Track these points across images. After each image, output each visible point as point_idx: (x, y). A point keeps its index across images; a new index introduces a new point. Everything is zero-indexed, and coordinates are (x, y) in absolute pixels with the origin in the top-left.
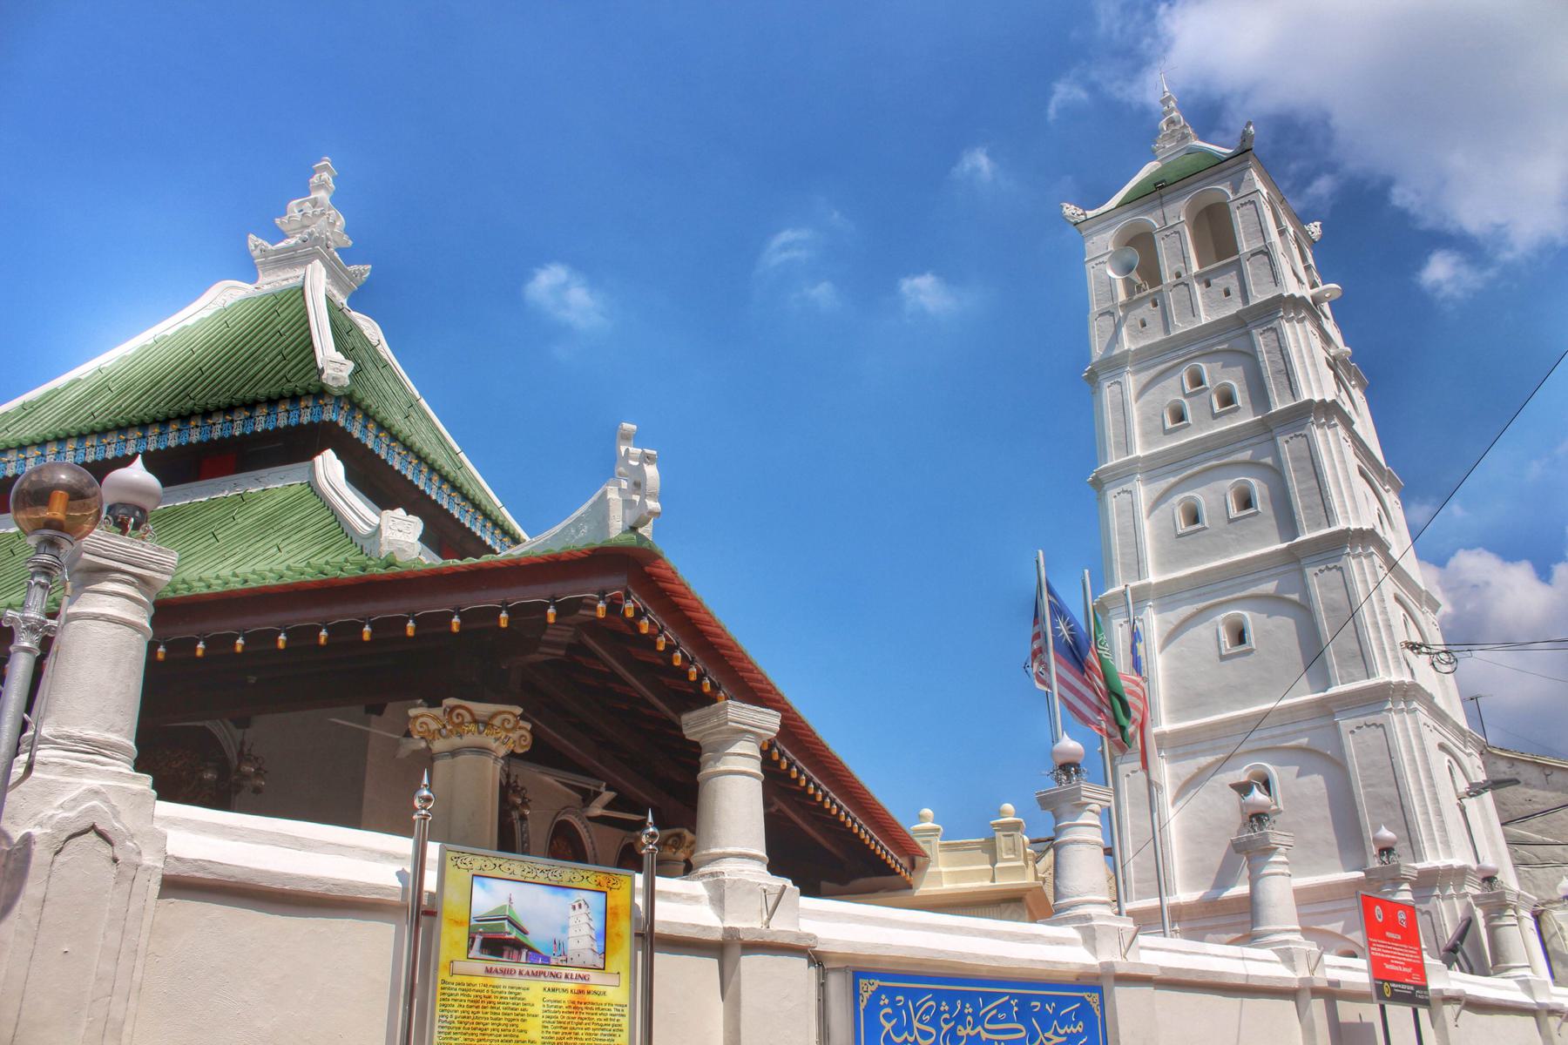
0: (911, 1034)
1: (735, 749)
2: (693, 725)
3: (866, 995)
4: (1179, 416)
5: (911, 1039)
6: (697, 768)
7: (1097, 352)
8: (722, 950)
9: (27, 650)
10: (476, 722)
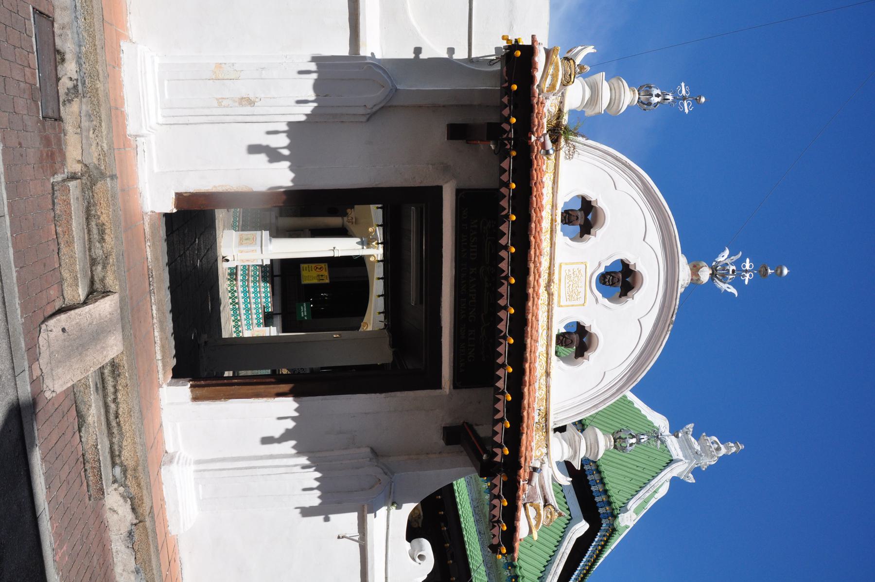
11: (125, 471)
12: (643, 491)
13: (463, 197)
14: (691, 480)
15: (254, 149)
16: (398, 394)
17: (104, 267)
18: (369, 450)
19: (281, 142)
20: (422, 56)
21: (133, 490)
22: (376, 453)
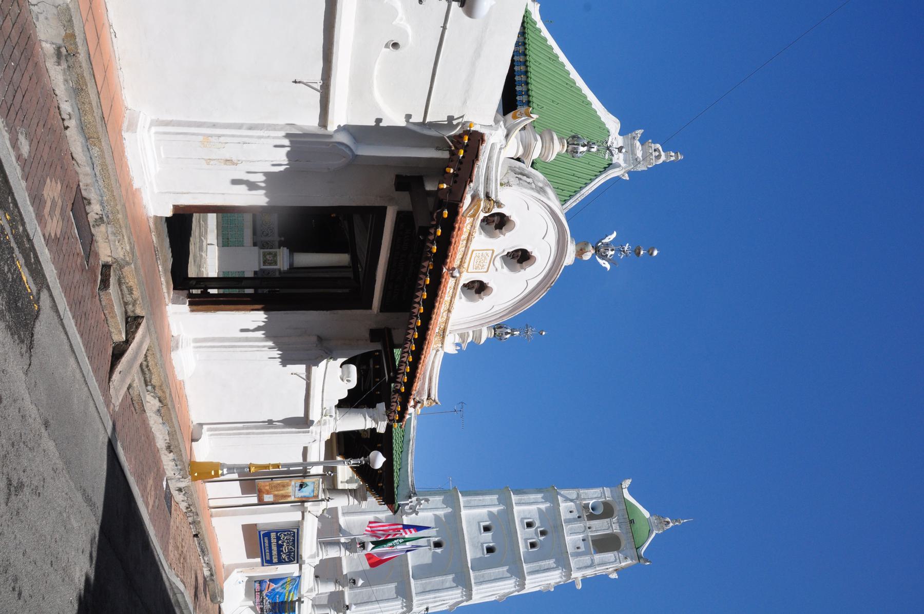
4: (529, 525)
7: (562, 492)
11: (154, 387)
12: (571, 201)
13: (403, 219)
14: (626, 177)
15: (235, 182)
16: (340, 312)
17: (134, 305)
18: (314, 339)
19: (260, 178)
20: (381, 125)
21: (160, 394)
22: (320, 339)
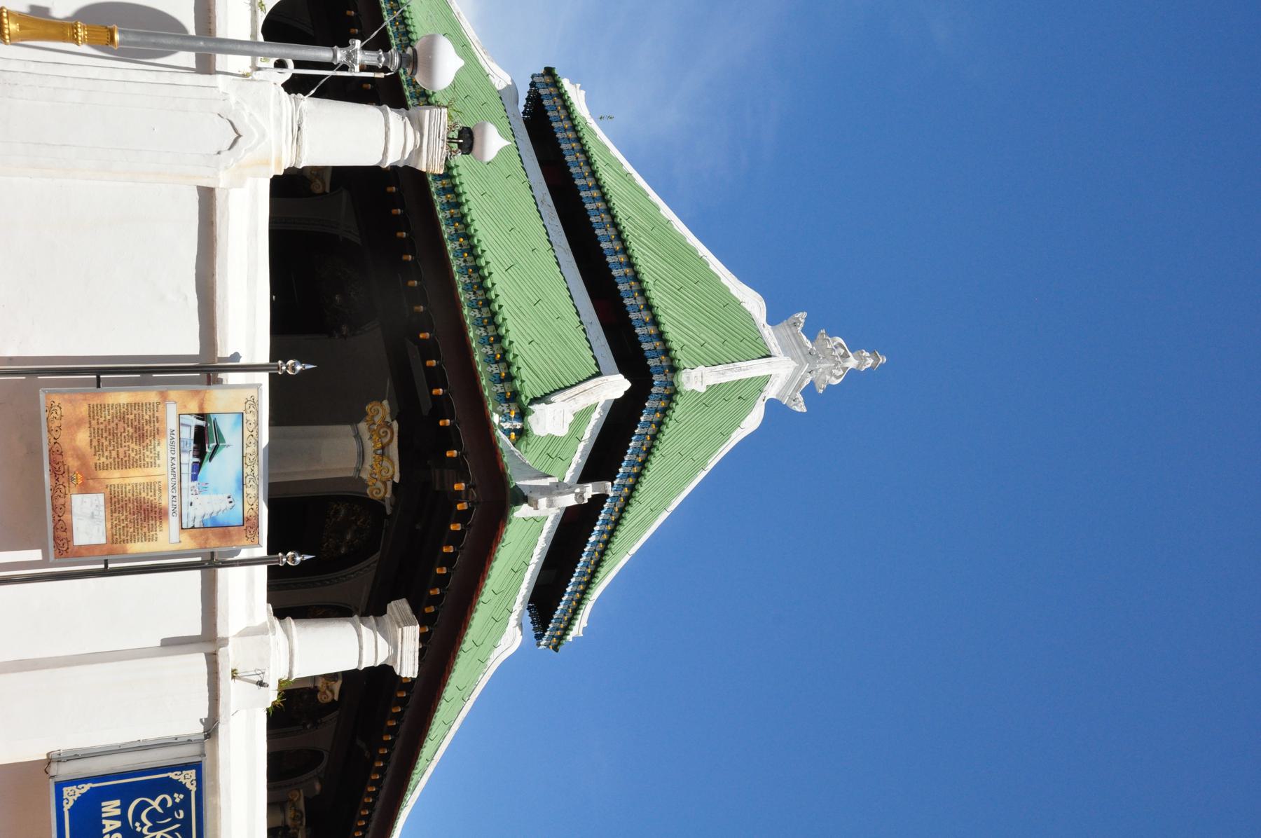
0: (150, 830)
1: (380, 639)
2: (399, 607)
3: (181, 779)
5: (145, 831)
6: (364, 614)
8: (208, 640)
9: (335, 56)
10: (383, 448)
14: (801, 408)
